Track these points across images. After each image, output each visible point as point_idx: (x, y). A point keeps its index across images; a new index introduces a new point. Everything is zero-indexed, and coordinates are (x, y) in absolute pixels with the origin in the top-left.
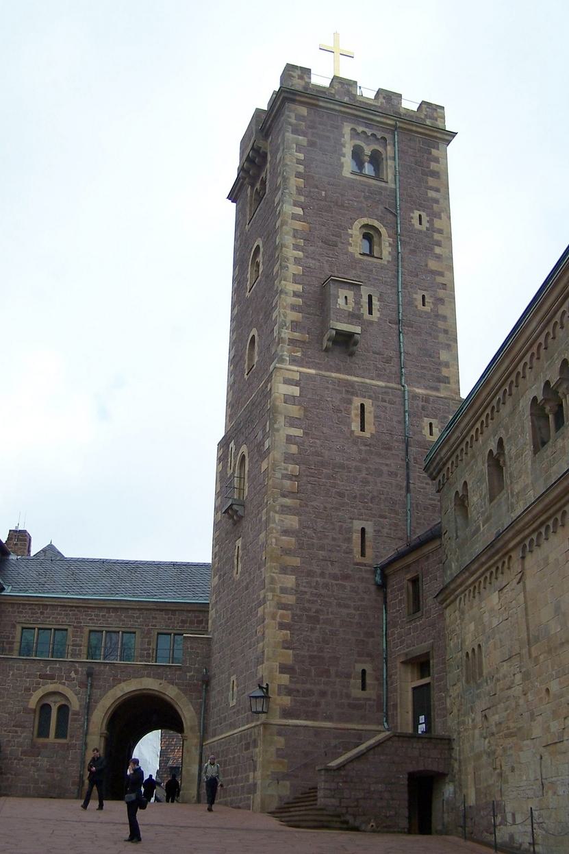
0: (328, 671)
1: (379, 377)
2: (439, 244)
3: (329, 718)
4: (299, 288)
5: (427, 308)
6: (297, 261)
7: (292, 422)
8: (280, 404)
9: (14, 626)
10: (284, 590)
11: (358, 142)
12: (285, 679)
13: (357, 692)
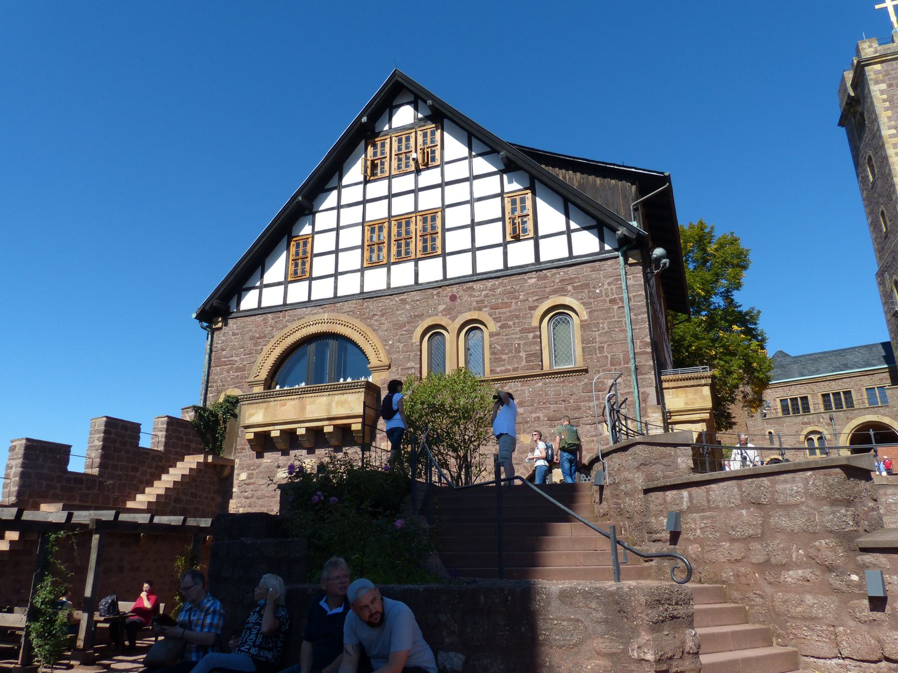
9: (775, 400)
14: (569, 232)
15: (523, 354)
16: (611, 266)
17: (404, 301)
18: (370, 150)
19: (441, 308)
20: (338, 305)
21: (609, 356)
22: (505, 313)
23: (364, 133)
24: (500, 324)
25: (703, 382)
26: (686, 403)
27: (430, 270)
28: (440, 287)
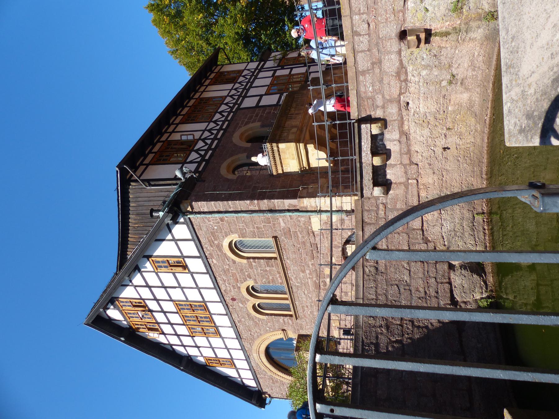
15: (268, 269)
18: (141, 330)
20: (247, 349)
21: (263, 224)
22: (240, 276)
23: (131, 336)
25: (275, 148)
26: (293, 159)
28: (227, 305)
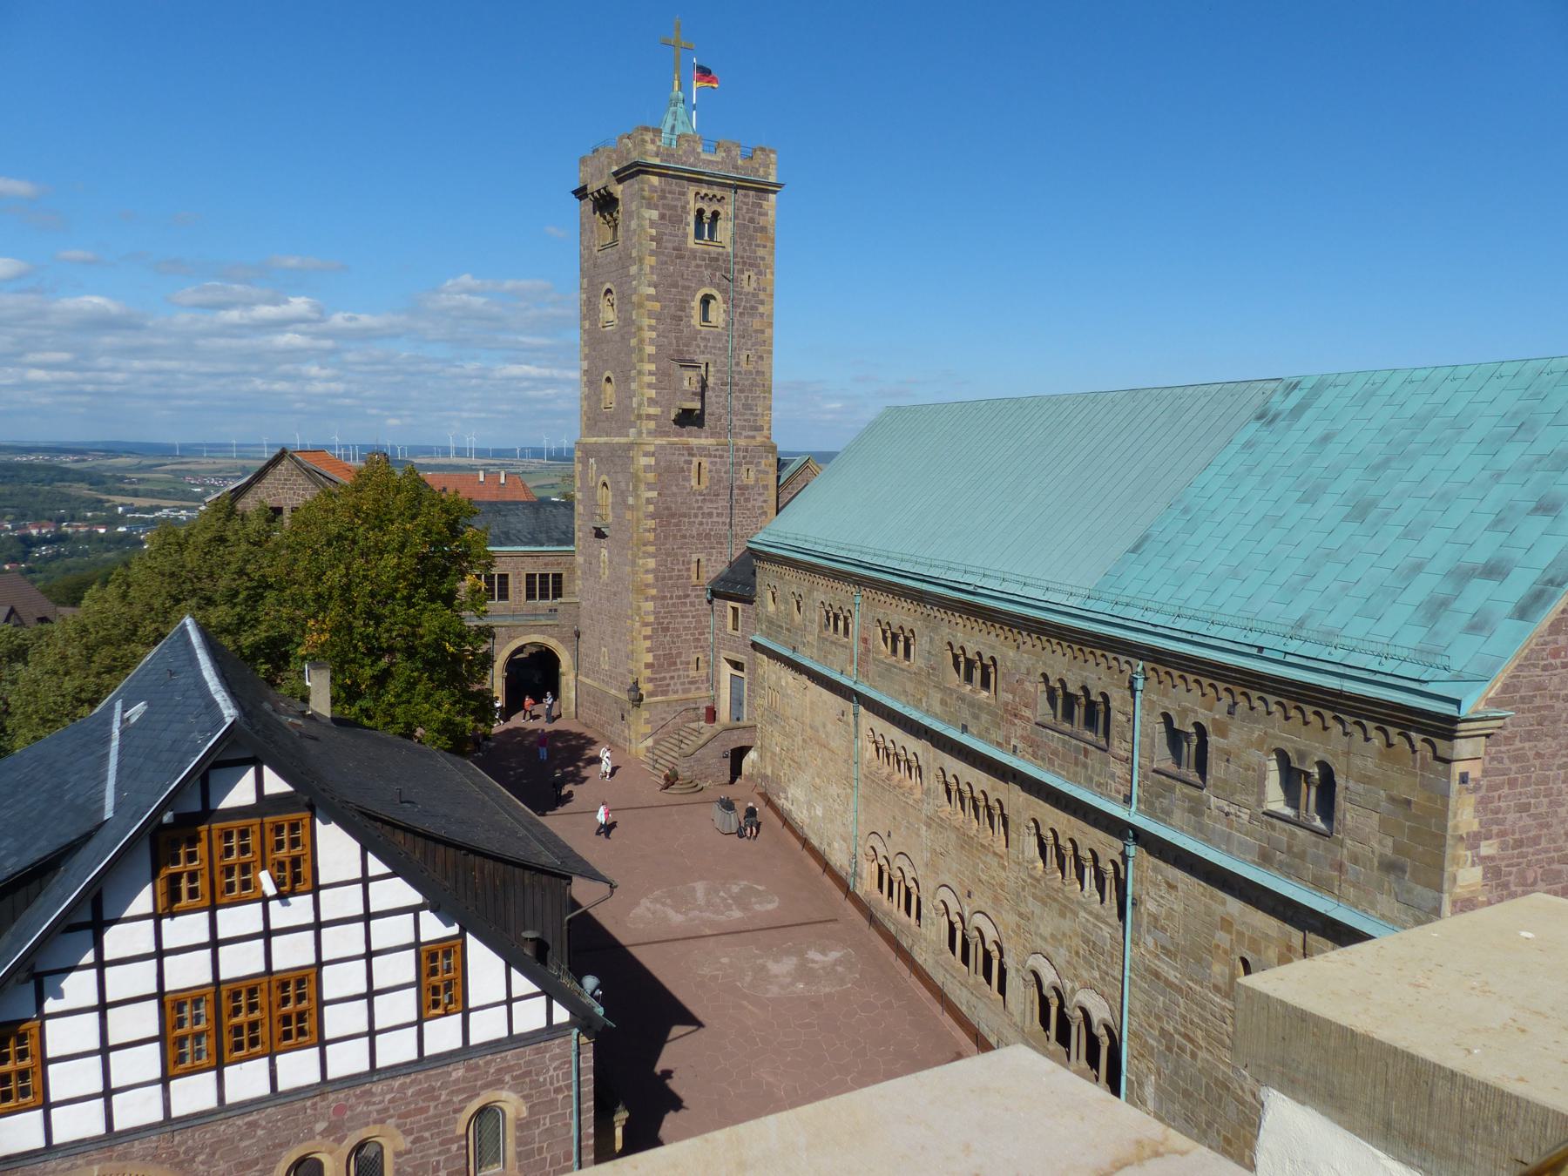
0: (675, 664)
1: (712, 435)
2: (762, 302)
3: (676, 692)
4: (653, 367)
5: (750, 367)
6: (652, 341)
7: (650, 487)
8: (642, 475)
10: (647, 613)
11: (700, 205)
12: (648, 673)
13: (693, 673)
14: (509, 1001)
16: (559, 1046)
17: (253, 1125)
19: (320, 1126)
24: (411, 1138)
27: (298, 1068)
